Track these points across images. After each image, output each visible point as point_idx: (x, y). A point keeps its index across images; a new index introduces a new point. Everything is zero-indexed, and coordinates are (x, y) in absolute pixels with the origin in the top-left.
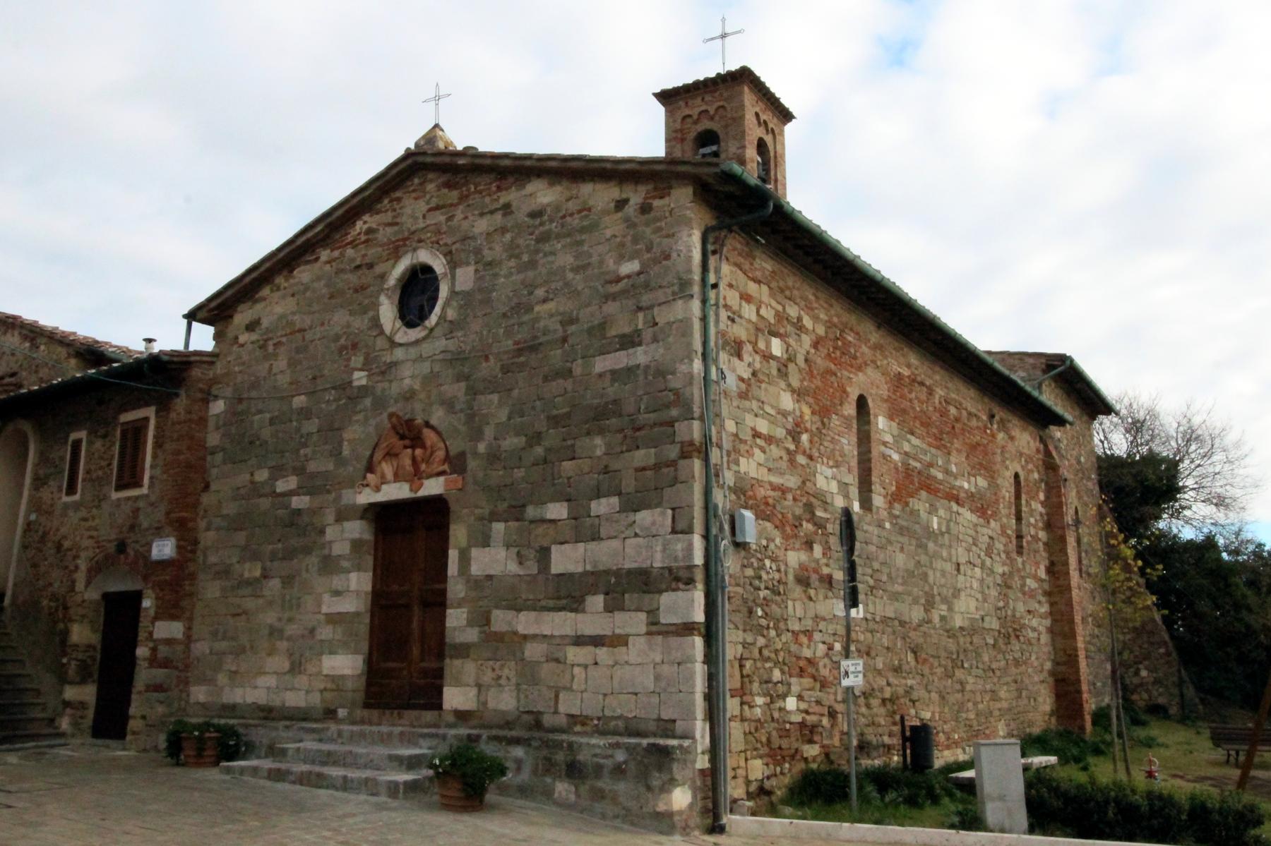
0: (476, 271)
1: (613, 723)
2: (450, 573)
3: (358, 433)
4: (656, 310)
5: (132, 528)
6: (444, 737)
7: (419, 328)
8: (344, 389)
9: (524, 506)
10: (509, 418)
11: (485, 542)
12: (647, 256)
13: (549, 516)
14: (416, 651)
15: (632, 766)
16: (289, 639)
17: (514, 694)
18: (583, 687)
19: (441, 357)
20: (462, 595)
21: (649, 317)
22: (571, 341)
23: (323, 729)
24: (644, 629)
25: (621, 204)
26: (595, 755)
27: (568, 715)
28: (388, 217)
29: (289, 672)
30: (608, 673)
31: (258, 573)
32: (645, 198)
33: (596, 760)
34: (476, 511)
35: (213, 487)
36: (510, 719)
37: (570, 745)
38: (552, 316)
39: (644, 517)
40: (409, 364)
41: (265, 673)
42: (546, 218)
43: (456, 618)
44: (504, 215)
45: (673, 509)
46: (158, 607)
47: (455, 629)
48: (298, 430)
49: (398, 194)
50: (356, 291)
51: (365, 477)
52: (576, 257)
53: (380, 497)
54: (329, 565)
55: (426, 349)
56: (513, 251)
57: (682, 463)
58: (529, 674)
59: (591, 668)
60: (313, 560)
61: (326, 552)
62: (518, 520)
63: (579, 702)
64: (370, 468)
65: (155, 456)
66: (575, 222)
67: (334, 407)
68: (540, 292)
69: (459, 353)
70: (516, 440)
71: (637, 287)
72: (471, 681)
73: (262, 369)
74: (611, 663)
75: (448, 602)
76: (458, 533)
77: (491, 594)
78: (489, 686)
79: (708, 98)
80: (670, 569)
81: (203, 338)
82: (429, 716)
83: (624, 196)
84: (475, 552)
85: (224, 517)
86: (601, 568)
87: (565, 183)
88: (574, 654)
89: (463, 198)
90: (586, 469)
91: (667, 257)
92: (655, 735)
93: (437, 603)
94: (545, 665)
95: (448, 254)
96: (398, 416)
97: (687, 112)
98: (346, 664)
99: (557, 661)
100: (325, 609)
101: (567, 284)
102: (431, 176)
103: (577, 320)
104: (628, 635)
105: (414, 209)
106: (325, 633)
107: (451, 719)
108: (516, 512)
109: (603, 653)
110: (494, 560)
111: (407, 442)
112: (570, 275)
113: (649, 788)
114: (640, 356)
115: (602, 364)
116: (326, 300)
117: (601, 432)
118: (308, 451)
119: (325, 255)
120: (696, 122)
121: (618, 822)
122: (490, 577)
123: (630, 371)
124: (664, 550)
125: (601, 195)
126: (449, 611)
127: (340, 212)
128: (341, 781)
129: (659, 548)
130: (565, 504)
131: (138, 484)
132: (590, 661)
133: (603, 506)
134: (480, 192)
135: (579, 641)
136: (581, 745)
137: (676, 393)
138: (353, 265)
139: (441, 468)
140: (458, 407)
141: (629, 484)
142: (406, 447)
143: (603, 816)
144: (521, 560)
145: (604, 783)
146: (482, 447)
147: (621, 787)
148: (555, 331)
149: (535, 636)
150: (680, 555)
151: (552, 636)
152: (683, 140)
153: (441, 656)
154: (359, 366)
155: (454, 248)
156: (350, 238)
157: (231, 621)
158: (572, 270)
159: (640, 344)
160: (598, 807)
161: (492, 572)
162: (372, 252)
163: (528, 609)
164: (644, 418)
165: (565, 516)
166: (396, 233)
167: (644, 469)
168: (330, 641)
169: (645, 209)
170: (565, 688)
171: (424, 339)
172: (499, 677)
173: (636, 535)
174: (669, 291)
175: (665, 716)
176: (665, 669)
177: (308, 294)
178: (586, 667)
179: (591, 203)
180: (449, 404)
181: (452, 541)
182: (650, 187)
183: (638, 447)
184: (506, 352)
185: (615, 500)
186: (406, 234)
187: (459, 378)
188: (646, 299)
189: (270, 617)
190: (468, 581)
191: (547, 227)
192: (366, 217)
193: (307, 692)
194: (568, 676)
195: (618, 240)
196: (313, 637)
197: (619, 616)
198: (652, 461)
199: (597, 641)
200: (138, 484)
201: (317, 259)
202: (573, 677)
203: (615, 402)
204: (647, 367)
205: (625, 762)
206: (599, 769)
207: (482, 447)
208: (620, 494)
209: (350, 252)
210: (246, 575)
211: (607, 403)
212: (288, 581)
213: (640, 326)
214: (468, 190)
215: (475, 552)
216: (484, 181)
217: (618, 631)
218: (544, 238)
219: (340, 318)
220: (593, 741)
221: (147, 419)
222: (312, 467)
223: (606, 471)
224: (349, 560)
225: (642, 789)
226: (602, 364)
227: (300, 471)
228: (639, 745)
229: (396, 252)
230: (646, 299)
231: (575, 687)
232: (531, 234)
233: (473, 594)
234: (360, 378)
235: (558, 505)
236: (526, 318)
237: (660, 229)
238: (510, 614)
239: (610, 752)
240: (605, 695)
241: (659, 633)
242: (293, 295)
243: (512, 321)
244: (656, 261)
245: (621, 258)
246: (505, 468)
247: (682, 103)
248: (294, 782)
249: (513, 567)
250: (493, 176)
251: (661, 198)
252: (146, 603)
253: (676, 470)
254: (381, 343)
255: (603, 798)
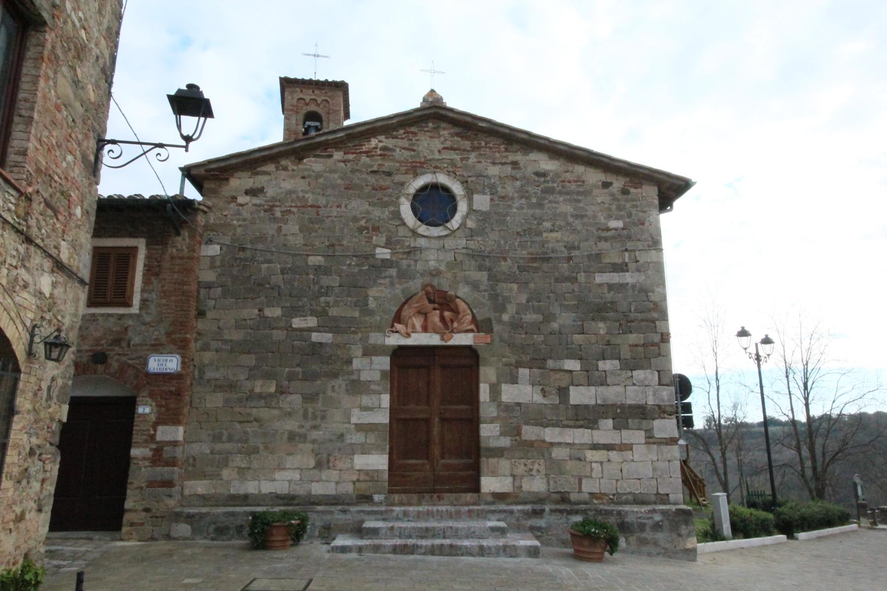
0: (492, 200)
1: (624, 497)
2: (482, 399)
3: (382, 294)
4: (637, 253)
5: (117, 342)
6: (512, 512)
7: (441, 228)
8: (367, 258)
9: (545, 360)
10: (528, 301)
11: (514, 380)
12: (627, 220)
13: (566, 368)
14: (437, 452)
15: (666, 523)
16: (314, 442)
17: (545, 480)
18: (600, 475)
19: (464, 251)
20: (495, 414)
21: (633, 257)
22: (575, 260)
23: (386, 511)
24: (644, 441)
25: (606, 185)
26: (640, 518)
27: (591, 494)
28: (406, 144)
29: (314, 468)
30: (619, 467)
31: (273, 389)
32: (624, 186)
33: (639, 520)
34: (504, 360)
35: (210, 315)
36: (542, 497)
37: (619, 513)
38: (558, 241)
39: (639, 374)
40: (433, 251)
41: (285, 469)
42: (548, 178)
43: (489, 432)
44: (513, 168)
45: (658, 371)
46: (159, 413)
47: (489, 437)
48: (316, 283)
49: (413, 129)
50: (374, 189)
51: (393, 326)
52: (575, 209)
53: (409, 342)
54: (357, 387)
55: (449, 243)
56: (523, 193)
57: (662, 345)
58: (555, 468)
59: (605, 465)
60: (340, 383)
61: (354, 377)
62: (540, 368)
63: (598, 485)
64: (398, 318)
65: (146, 281)
66: (573, 187)
67: (356, 270)
68: (548, 225)
69: (480, 252)
70: (535, 316)
71: (621, 237)
72: (507, 472)
73: (270, 229)
74: (621, 460)
75: (482, 419)
76: (488, 373)
77: (515, 416)
78: (522, 477)
79: (316, 92)
80: (659, 406)
81: (192, 193)
82: (469, 497)
83: (609, 180)
84: (504, 387)
85: (226, 342)
86: (610, 403)
87: (562, 160)
88: (590, 455)
89: (474, 149)
90: (593, 341)
91: (643, 224)
92: (655, 503)
93: (473, 421)
94: (569, 462)
95: (464, 183)
96: (433, 287)
97: (301, 96)
98: (379, 462)
99: (580, 459)
100: (354, 420)
101: (568, 224)
102: (443, 125)
103: (579, 248)
104: (632, 444)
105: (430, 144)
106: (357, 438)
107: (490, 499)
108: (538, 362)
109: (613, 455)
110: (522, 392)
111: (436, 306)
112: (571, 220)
113: (680, 535)
114: (629, 278)
115: (600, 278)
116: (343, 189)
117: (603, 319)
118: (330, 299)
119: (338, 155)
120: (307, 104)
121: (660, 558)
122: (519, 404)
123: (622, 287)
124: (654, 395)
125: (594, 177)
126: (482, 426)
127: (362, 128)
128: (477, 549)
129: (651, 393)
130: (579, 361)
131: (128, 305)
132: (605, 459)
133: (606, 365)
134: (491, 148)
135: (595, 447)
136: (627, 512)
137: (655, 304)
138: (370, 170)
139: (470, 327)
140: (482, 288)
141: (626, 353)
142: (435, 309)
143: (649, 554)
144: (544, 393)
145: (648, 535)
146: (506, 317)
147: (660, 536)
148: (562, 252)
149: (559, 444)
150: (666, 398)
151: (574, 444)
152: (297, 113)
153: (478, 456)
154: (383, 245)
155: (469, 180)
156: (364, 149)
157: (238, 426)
158: (572, 216)
159: (627, 271)
160: (645, 549)
161: (521, 401)
162: (388, 165)
163: (554, 426)
164: (632, 316)
165: (579, 368)
166: (412, 156)
167: (636, 346)
168: (362, 444)
169: (625, 192)
170: (586, 477)
171: (446, 236)
172: (531, 470)
173: (634, 384)
174: (646, 244)
175: (661, 491)
176: (660, 464)
177: (321, 180)
178: (601, 463)
179: (584, 178)
180: (475, 286)
181: (482, 378)
182: (628, 179)
183: (631, 332)
184: (521, 258)
185: (616, 362)
186: (423, 160)
187: (480, 268)
188: (630, 245)
189: (291, 425)
190: (499, 406)
191: (550, 185)
192: (382, 138)
193: (337, 483)
194: (588, 469)
195: (607, 206)
196: (343, 441)
197: (625, 432)
198: (642, 342)
199: (609, 447)
200: (128, 305)
201: (330, 156)
202: (592, 470)
203: (612, 302)
204: (634, 286)
205: (661, 521)
206: (642, 527)
207: (506, 317)
208: (619, 359)
209: (364, 159)
210: (258, 390)
211: (605, 303)
212: (309, 398)
213: (627, 260)
214: (480, 144)
215: (504, 387)
216: (493, 142)
217: (624, 441)
218: (549, 191)
219: (357, 206)
220: (636, 509)
221: (135, 249)
222: (334, 312)
223: (608, 344)
224: (379, 385)
225: (674, 536)
226: (600, 278)
227: (321, 314)
228: (671, 510)
229: (416, 169)
230: (630, 245)
231: (594, 475)
232: (538, 186)
233: (505, 415)
234: (383, 253)
235: (572, 361)
236: (537, 239)
237: (636, 206)
238: (536, 430)
239: (650, 515)
240: (617, 480)
241: (654, 443)
242: (303, 178)
243: (525, 239)
244: (634, 224)
245: (610, 217)
246: (526, 333)
247: (298, 90)
248: (424, 554)
249: (538, 398)
250: (501, 140)
251: (636, 188)
252: (143, 409)
253: (659, 349)
254: (402, 231)
255: (648, 543)
